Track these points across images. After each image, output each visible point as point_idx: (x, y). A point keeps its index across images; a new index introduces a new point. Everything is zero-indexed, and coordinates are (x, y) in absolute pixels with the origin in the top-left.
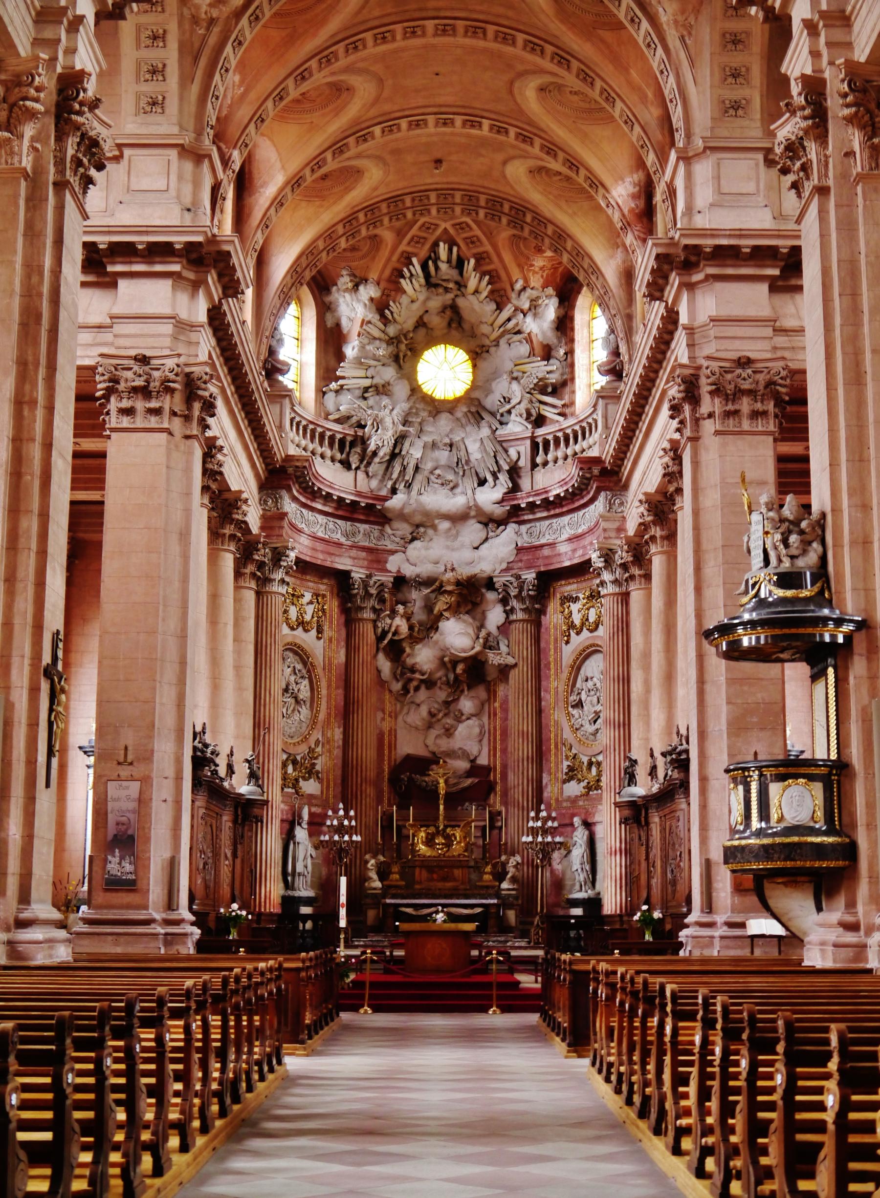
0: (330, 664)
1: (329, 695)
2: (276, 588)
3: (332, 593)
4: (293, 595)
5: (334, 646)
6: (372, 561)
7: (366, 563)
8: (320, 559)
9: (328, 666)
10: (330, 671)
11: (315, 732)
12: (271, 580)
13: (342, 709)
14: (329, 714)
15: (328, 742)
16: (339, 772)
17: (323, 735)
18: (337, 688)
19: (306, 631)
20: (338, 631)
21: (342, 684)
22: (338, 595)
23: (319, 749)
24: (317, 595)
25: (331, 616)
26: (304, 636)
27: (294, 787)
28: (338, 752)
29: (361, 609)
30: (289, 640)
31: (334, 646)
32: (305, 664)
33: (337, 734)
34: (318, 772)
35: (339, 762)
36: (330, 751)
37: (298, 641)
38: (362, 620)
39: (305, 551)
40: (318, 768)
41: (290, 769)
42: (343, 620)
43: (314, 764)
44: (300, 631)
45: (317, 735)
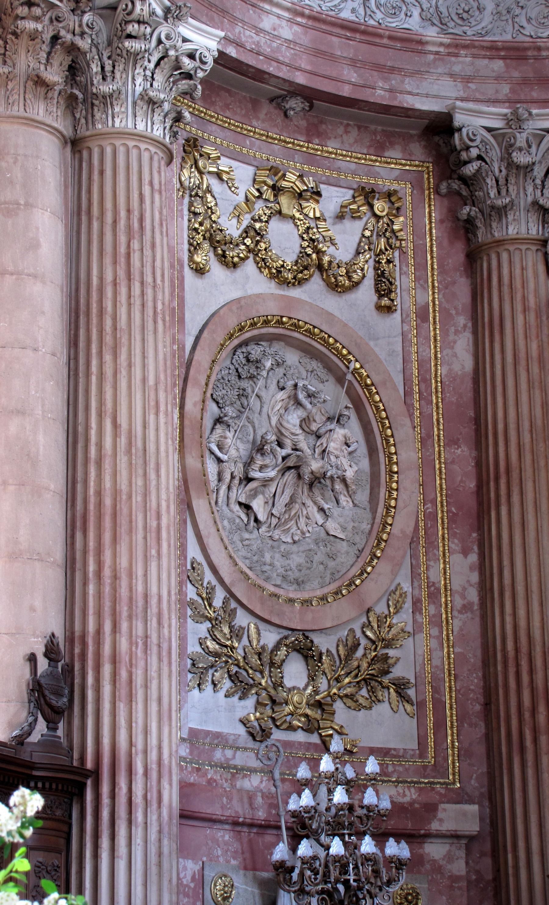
0: (424, 380)
1: (424, 467)
2: (126, 119)
3: (417, 185)
4: (276, 189)
5: (432, 329)
6: (525, 82)
7: (505, 89)
8: (347, 81)
9: (419, 381)
10: (425, 398)
11: (383, 567)
12: (108, 100)
13: (472, 503)
14: (431, 517)
15: (433, 595)
16: (475, 681)
17: (414, 575)
18: (452, 442)
19: (335, 287)
20: (446, 286)
21: (468, 430)
22: (437, 192)
23: (403, 619)
24: (368, 194)
25: (420, 251)
26: (332, 303)
27: (311, 727)
28: (464, 624)
29: (501, 212)
30: (272, 309)
31: (432, 329)
32: (340, 380)
33: (458, 571)
34: (400, 686)
35: (474, 655)
36: (436, 621)
37: (303, 315)
38: (500, 242)
39: (286, 55)
40: (397, 672)
41: (295, 673)
42: (458, 256)
43: (383, 664)
44: (314, 290)
45: (391, 576)
